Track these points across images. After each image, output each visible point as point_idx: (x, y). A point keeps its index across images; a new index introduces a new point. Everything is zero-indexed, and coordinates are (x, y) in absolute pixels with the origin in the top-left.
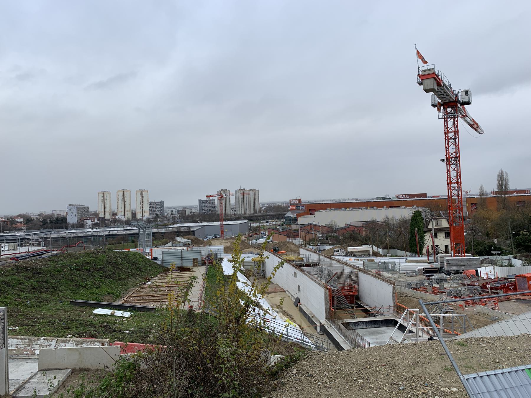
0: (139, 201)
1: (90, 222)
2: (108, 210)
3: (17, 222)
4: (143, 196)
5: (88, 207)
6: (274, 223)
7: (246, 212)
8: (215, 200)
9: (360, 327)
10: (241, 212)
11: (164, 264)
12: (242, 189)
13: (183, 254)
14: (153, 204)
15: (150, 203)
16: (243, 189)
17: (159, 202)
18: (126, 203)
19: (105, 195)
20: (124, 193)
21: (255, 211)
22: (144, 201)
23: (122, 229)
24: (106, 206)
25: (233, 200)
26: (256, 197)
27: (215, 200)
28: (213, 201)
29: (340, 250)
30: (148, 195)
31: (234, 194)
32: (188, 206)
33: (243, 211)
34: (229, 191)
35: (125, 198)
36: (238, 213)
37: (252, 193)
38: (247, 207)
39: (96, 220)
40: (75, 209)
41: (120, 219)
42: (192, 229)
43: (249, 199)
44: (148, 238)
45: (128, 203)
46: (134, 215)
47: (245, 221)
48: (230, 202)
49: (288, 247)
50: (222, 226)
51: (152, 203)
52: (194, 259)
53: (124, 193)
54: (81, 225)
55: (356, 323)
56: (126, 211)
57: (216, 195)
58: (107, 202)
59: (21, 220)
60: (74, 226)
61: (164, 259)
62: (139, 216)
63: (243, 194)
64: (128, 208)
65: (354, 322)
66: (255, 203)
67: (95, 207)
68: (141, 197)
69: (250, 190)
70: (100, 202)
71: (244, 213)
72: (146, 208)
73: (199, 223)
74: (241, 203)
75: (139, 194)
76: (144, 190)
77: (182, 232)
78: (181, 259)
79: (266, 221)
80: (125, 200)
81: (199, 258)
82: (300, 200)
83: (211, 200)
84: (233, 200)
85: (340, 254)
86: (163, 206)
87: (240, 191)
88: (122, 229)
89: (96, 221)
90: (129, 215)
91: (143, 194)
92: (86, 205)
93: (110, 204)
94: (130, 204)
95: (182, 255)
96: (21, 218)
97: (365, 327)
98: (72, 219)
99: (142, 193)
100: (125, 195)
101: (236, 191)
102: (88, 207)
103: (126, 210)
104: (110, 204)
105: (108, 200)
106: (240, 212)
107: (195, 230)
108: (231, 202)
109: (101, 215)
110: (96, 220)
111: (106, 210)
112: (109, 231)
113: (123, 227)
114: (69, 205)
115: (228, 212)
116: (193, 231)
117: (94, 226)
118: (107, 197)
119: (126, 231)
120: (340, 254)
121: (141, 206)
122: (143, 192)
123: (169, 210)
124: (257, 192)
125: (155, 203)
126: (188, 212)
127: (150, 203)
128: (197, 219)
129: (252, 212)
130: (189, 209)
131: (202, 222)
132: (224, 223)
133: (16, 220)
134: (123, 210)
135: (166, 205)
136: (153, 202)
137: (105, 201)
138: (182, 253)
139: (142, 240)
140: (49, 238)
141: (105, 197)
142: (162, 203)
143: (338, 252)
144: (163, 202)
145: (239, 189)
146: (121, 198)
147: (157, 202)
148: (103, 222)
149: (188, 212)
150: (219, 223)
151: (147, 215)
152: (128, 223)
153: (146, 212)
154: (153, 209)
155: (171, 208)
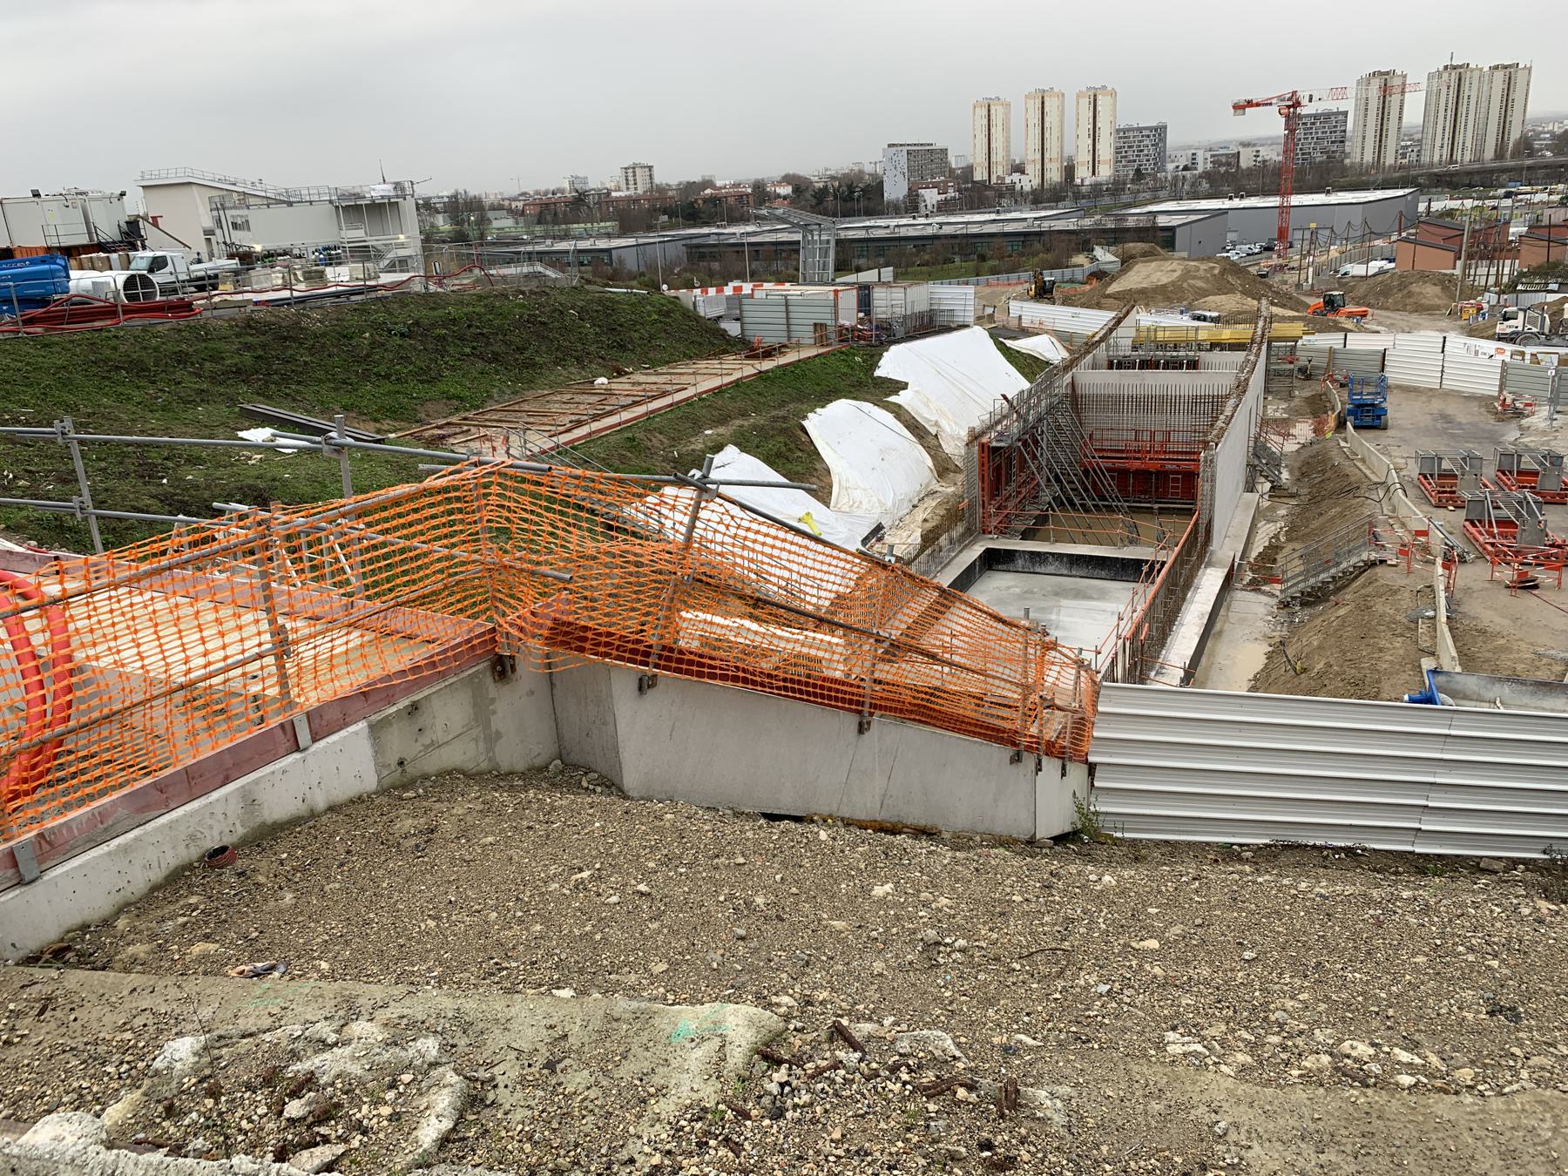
0: (1086, 125)
1: (931, 196)
2: (1000, 159)
3: (778, 196)
4: (1099, 108)
5: (944, 151)
6: (1537, 198)
7: (1458, 156)
8: (1345, 114)
9: (1051, 569)
10: (1436, 159)
11: (747, 333)
12: (1455, 68)
13: (791, 308)
14: (1131, 134)
15: (1118, 131)
16: (1461, 67)
17: (1150, 129)
18: (1047, 135)
19: (992, 111)
20: (1043, 103)
21: (1500, 154)
22: (1099, 125)
23: (993, 216)
24: (993, 145)
25: (1413, 111)
26: (1517, 96)
27: (1345, 114)
28: (1340, 117)
29: (1521, 315)
30: (1115, 105)
31: (1424, 86)
32: (1259, 139)
33: (1446, 152)
34: (1405, 76)
35: (1047, 119)
36: (1425, 159)
37: (1499, 76)
38: (1467, 137)
39: (951, 190)
40: (903, 159)
41: (1018, 187)
42: (1162, 221)
43: (1483, 103)
44: (826, 255)
45: (1055, 133)
46: (1070, 171)
47: (1400, 192)
48: (1400, 118)
49: (1410, 295)
50: (1284, 210)
51: (1129, 130)
52: (815, 325)
53: (1043, 103)
54: (912, 205)
55: (1036, 557)
56: (1046, 160)
57: (1274, 101)
58: (997, 133)
59: (786, 190)
60: (896, 210)
61: (792, 321)
62: (1083, 174)
63: (1386, 90)
64: (1052, 152)
65: (1032, 553)
66: (1508, 119)
67: (964, 150)
68: (1091, 114)
69: (1496, 67)
70: (978, 133)
71: (1452, 161)
72: (1106, 150)
73: (1231, 198)
74: (1443, 123)
75: (1085, 104)
76: (1104, 87)
77: (1128, 230)
78: (784, 321)
79: (1503, 191)
80: (1047, 125)
81: (829, 322)
82: (1160, 131)
83: (1334, 114)
84: (1413, 111)
85: (1520, 329)
86: (1163, 140)
87: (1445, 75)
88: (993, 216)
89: (951, 193)
90: (1054, 175)
91: (1099, 103)
92: (939, 145)
93: (1008, 140)
94: (1061, 138)
95: (787, 312)
96: (789, 184)
97: (1065, 572)
98: (895, 190)
99: (1095, 100)
100: (1046, 109)
101: (1358, 83)
102: (944, 151)
103: (1047, 156)
104: (1008, 140)
105: (1000, 128)
106: (1435, 154)
107: (1179, 226)
108: (1405, 120)
109: (979, 175)
110: (951, 190)
111: (993, 159)
112: (941, 225)
113: (998, 212)
114: (890, 146)
115: (1389, 160)
116: (1172, 229)
117: (944, 207)
118: (997, 119)
119: (779, 235)
120: (1520, 329)
121: (1090, 141)
122: (1099, 97)
123: (1183, 153)
124: (1520, 79)
125: (1140, 130)
126: (1246, 161)
127: (1123, 133)
128: (1251, 185)
129: (1489, 153)
130: (1250, 149)
131: (1242, 197)
132: (1296, 200)
133: (778, 190)
134: (1039, 156)
135: (1172, 139)
136: (1133, 130)
137: (993, 130)
138: (787, 305)
139: (809, 260)
140: (743, 244)
141: (993, 117)
142: (1160, 131)
143: (1511, 322)
144: (1165, 127)
145: (1446, 68)
146: (1035, 119)
147: (1146, 128)
148: (976, 194)
149: (1246, 161)
150: (1274, 201)
151: (1105, 172)
152: (1038, 198)
153: (1105, 162)
154: (1130, 153)
155: (1190, 148)
